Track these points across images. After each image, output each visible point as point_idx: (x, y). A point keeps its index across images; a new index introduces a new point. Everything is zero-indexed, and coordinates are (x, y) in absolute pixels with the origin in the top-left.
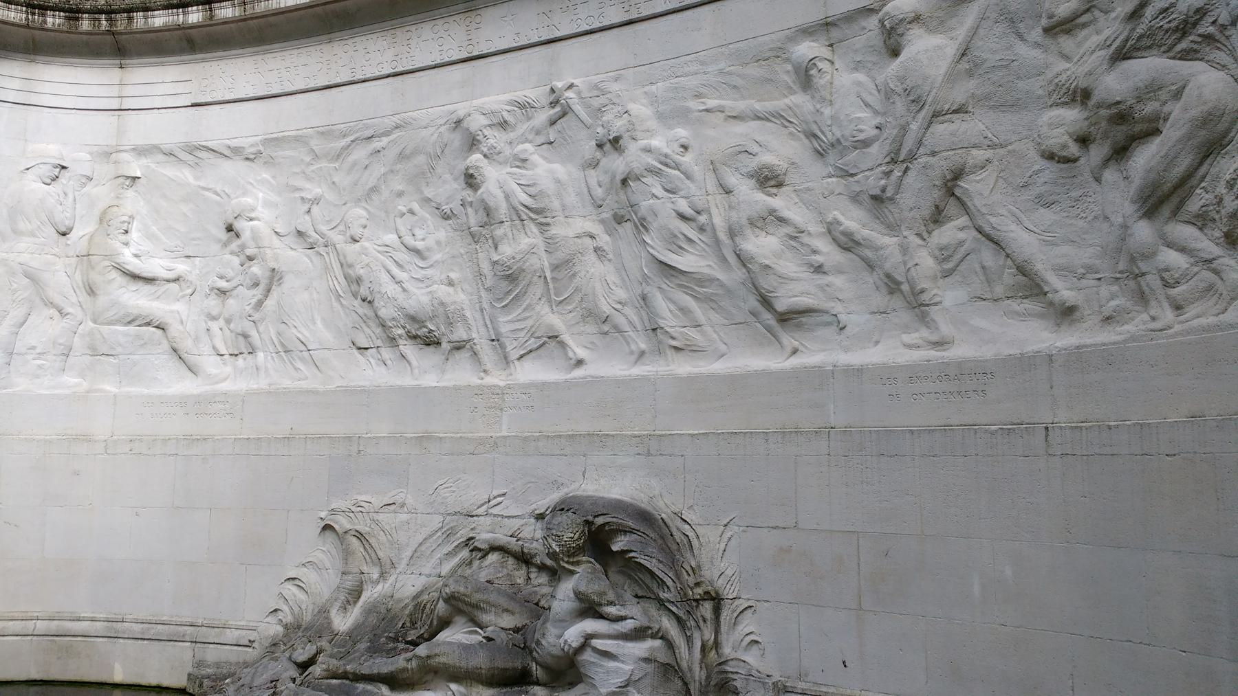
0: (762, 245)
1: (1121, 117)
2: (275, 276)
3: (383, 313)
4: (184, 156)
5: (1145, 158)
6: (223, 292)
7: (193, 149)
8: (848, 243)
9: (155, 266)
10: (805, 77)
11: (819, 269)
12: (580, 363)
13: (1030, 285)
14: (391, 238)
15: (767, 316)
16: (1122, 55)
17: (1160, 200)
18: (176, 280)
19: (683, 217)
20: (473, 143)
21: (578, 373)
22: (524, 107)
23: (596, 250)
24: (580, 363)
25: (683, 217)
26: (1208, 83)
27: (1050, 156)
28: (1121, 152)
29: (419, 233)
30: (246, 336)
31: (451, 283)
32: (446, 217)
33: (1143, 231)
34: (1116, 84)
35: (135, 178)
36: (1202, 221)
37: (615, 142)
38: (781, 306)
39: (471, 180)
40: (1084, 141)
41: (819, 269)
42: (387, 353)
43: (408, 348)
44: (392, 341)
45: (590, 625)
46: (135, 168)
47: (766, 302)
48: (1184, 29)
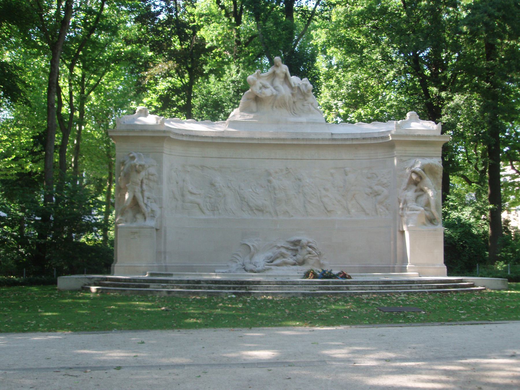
0: (325, 200)
1: (376, 192)
2: (225, 196)
3: (251, 204)
4: (200, 168)
5: (379, 198)
6: (210, 197)
7: (202, 167)
8: (339, 201)
9: (194, 191)
10: (332, 175)
11: (333, 204)
12: (292, 216)
13: (364, 210)
14: (251, 190)
15: (326, 211)
16: (377, 185)
17: (381, 203)
18: (200, 194)
19: (313, 194)
20: (269, 174)
21: (291, 218)
22: (281, 170)
23: (295, 197)
24: (292, 216)
25: (313, 194)
26: (386, 192)
27: (366, 194)
28: (375, 196)
29: (257, 190)
30: (217, 207)
31: (265, 200)
32: (262, 187)
33: (378, 206)
34: (376, 188)
35: (188, 171)
36: (384, 206)
37: (300, 180)
38: (329, 209)
39: (269, 181)
40: (371, 193)
41: (333, 204)
42: (250, 212)
43: (255, 211)
44: (252, 210)
45: (309, 255)
46: (189, 169)
47: (326, 209)
48: (384, 184)
